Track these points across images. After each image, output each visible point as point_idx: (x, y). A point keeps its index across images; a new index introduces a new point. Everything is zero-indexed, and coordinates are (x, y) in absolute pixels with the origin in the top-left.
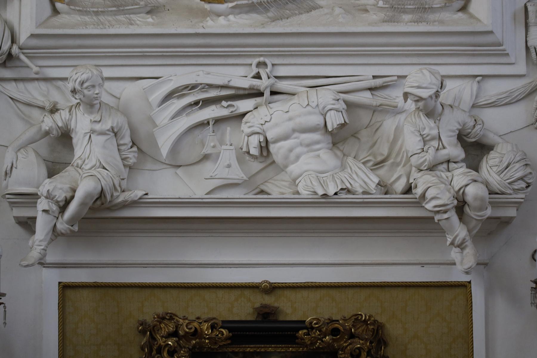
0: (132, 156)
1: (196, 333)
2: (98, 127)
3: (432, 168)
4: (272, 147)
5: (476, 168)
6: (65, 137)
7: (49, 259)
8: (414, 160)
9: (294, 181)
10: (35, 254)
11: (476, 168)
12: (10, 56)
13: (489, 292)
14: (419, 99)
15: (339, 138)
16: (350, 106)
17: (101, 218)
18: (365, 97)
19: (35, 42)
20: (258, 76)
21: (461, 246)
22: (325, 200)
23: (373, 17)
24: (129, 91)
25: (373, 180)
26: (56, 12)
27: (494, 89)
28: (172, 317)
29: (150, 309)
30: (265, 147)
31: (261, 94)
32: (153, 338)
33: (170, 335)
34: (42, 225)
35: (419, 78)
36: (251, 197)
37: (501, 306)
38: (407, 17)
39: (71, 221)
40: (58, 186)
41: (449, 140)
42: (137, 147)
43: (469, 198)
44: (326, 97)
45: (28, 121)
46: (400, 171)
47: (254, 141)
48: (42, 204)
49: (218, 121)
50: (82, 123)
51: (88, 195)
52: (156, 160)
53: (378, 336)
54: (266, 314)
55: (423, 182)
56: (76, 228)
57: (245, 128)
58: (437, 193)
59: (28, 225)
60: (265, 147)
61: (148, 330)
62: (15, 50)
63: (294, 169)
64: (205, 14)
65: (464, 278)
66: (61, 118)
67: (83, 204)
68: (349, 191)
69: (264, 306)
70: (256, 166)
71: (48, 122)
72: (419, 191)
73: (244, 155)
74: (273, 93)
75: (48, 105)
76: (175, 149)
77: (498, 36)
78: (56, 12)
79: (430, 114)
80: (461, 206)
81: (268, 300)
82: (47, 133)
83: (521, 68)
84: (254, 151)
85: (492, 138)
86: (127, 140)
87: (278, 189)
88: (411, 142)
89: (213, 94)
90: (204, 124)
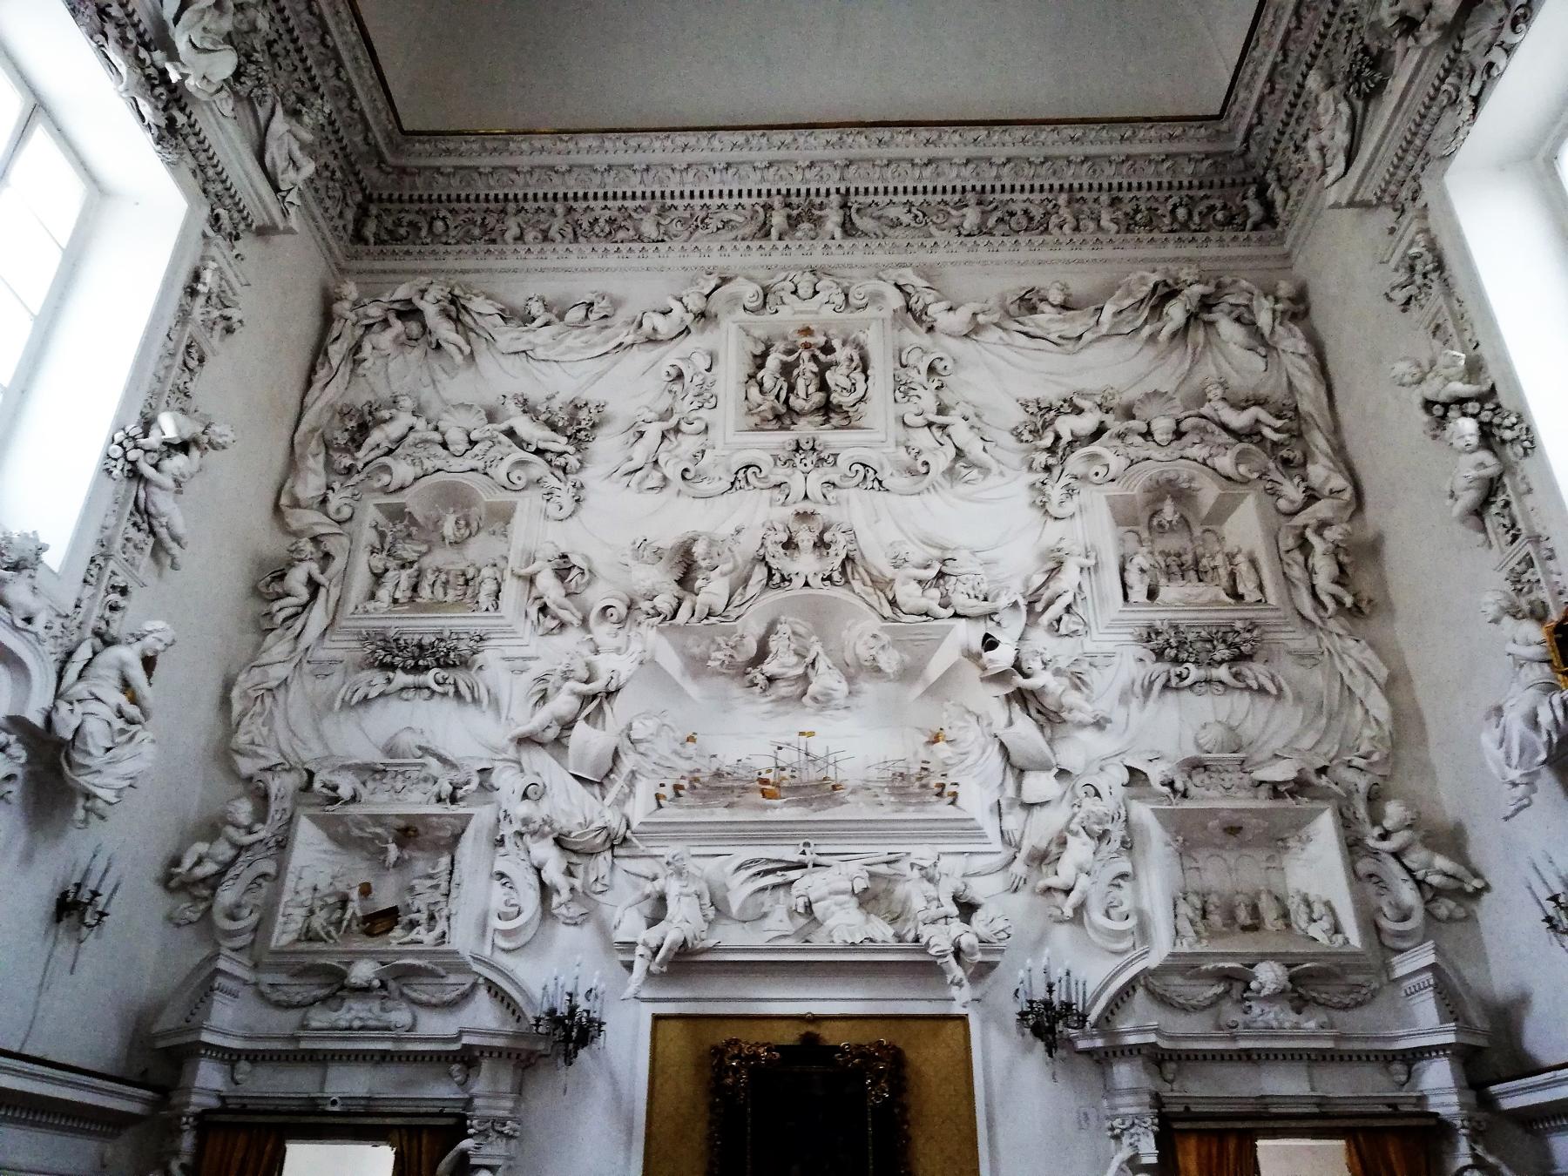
0: (711, 913)
1: (756, 1056)
2: (685, 890)
3: (934, 922)
4: (814, 907)
5: (968, 923)
6: (662, 899)
7: (644, 994)
8: (920, 916)
9: (830, 934)
10: (630, 991)
11: (968, 923)
12: (625, 839)
13: (984, 1022)
14: (922, 868)
15: (867, 900)
16: (872, 876)
17: (684, 962)
18: (883, 869)
19: (643, 828)
20: (804, 853)
21: (959, 984)
22: (853, 948)
23: (887, 809)
24: (710, 865)
25: (890, 931)
26: (660, 806)
27: (978, 863)
28: (737, 1041)
29: (723, 1035)
30: (809, 907)
31: (805, 866)
32: (721, 1061)
33: (733, 1058)
34: (640, 966)
35: (923, 852)
36: (800, 945)
37: (994, 1034)
38: (911, 809)
39: (661, 964)
40: (653, 936)
41: (947, 901)
42: (718, 907)
43: (963, 945)
44: (854, 867)
45: (636, 887)
46: (910, 925)
47: (801, 902)
48: (640, 950)
49: (775, 887)
50: (673, 888)
51: (674, 943)
52: (729, 917)
53: (896, 1058)
54: (810, 1040)
55: (926, 933)
56: (665, 969)
57: (795, 890)
58: (939, 939)
59: (629, 966)
60: (809, 907)
61: (718, 1052)
62: (629, 834)
63: (830, 923)
64: (765, 808)
65: (962, 1011)
66: (658, 885)
67: (670, 950)
68: (871, 940)
69: (808, 1034)
70: (802, 921)
71: (649, 888)
72: (923, 941)
73: (792, 913)
74: (815, 865)
75: (651, 875)
76: (743, 908)
77: (980, 821)
78: (660, 806)
79: (931, 880)
80: (958, 952)
81: (811, 1028)
82: (648, 896)
83: (997, 845)
84: (801, 910)
85: (979, 899)
86: (707, 900)
87: (819, 940)
88: (918, 903)
89: (771, 866)
90: (764, 889)
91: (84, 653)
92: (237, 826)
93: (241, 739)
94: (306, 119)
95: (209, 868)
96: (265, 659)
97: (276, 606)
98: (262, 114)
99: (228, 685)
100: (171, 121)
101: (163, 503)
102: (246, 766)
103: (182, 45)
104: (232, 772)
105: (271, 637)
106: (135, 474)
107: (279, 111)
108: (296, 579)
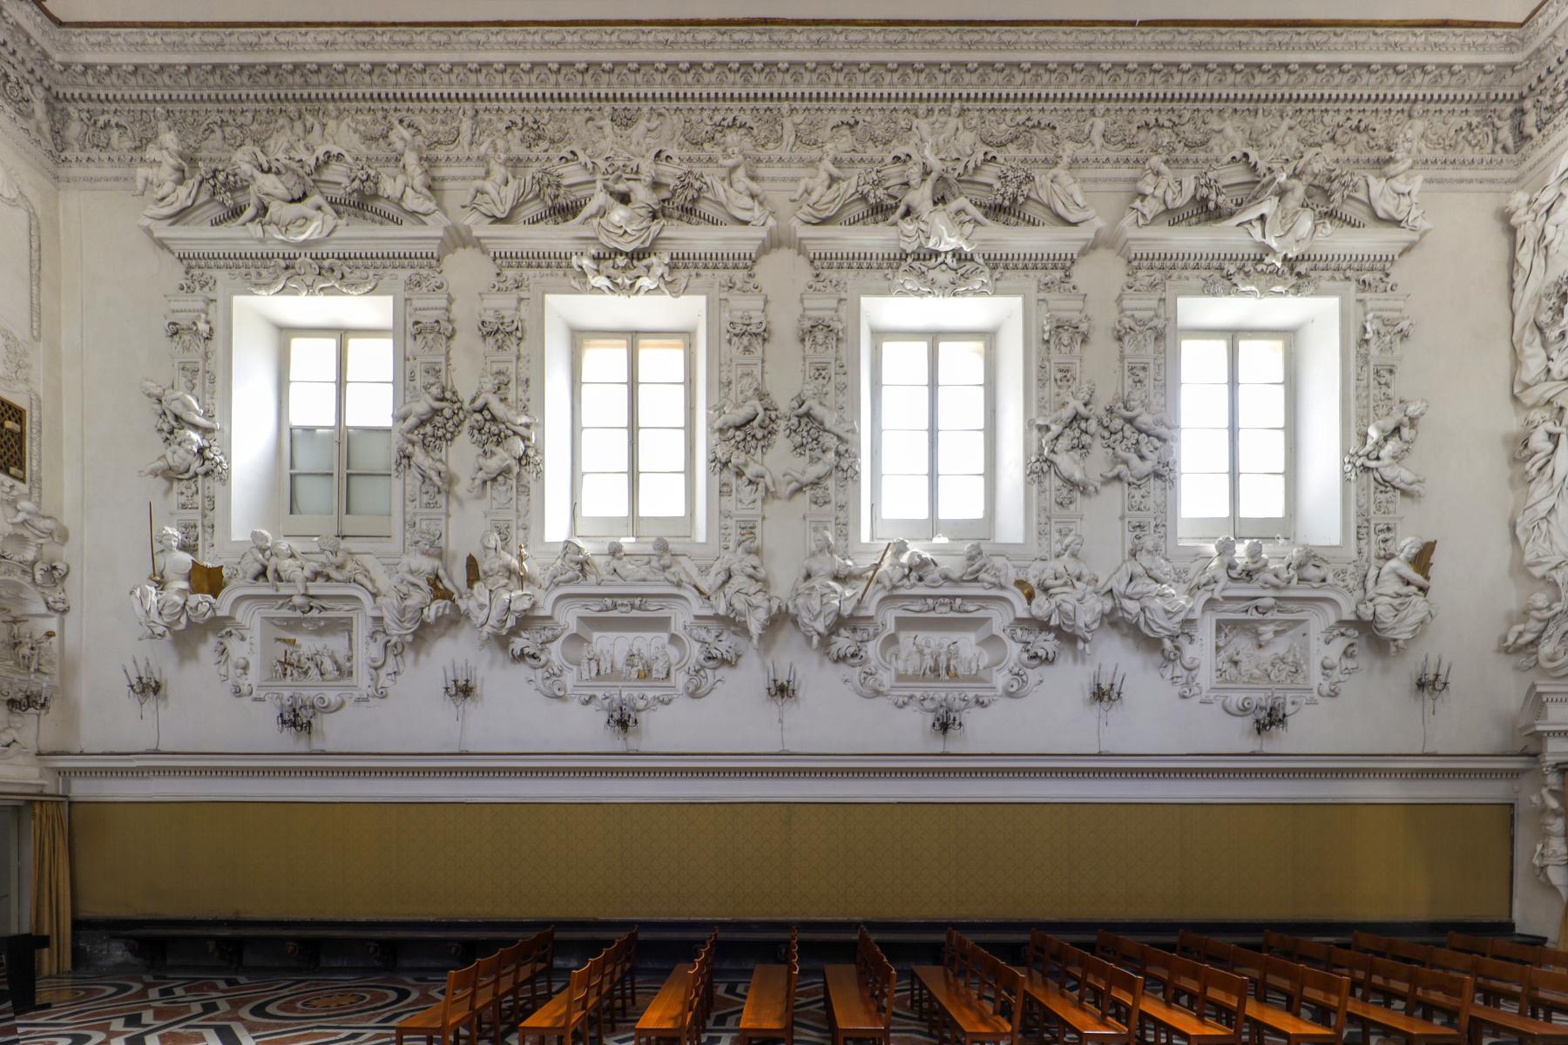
91: (1373, 573)
92: (1539, 609)
93: (1529, 558)
94: (1398, 156)
95: (1528, 637)
96: (1531, 502)
97: (1528, 465)
98: (1361, 195)
99: (1513, 526)
100: (1299, 274)
101: (1389, 473)
102: (1538, 572)
103: (1274, 244)
104: (1531, 577)
105: (1533, 486)
106: (1367, 469)
107: (1372, 180)
108: (1539, 441)
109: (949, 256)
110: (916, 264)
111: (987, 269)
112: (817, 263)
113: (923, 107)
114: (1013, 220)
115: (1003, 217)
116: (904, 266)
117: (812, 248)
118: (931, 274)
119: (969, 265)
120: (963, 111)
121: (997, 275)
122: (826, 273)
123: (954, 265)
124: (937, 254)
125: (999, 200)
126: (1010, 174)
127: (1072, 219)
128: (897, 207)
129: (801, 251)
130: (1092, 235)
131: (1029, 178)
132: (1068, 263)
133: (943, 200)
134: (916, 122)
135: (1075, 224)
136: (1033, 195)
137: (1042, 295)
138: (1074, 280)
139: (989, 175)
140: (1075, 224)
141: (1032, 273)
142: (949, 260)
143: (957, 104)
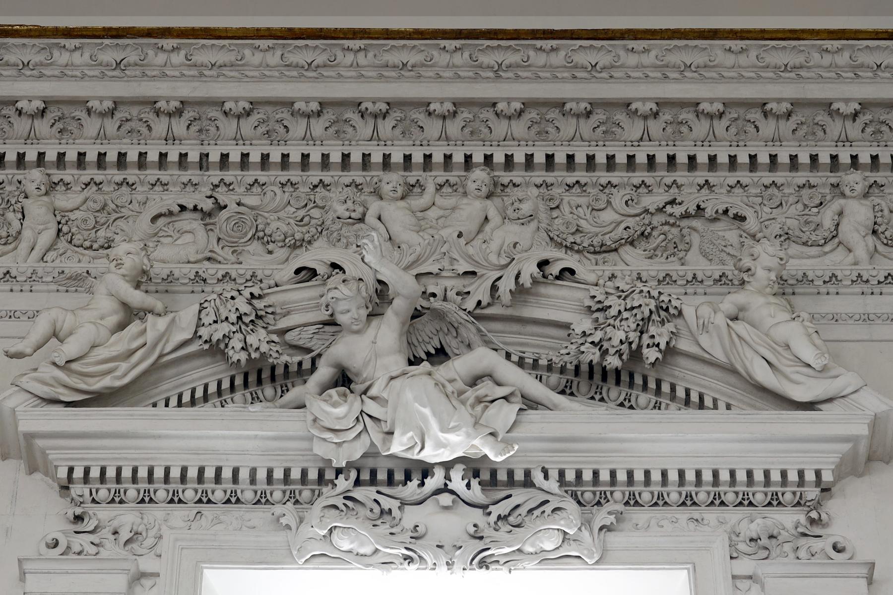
109: (457, 475)
110: (365, 494)
111: (570, 505)
112: (77, 489)
113: (392, 181)
114: (643, 398)
115: (615, 393)
116: (330, 495)
117: (62, 459)
118: (411, 516)
119: (519, 496)
120: (495, 191)
121: (602, 517)
122: (103, 513)
123: (476, 493)
124: (426, 471)
125: (593, 355)
126: (616, 305)
127: (800, 394)
128: (314, 368)
129: (35, 464)
130: (863, 430)
131: (666, 312)
132: (812, 493)
133: (440, 355)
134: (375, 206)
135: (810, 406)
136: (684, 345)
137: (744, 566)
138: (837, 532)
139: (560, 304)
140: (810, 406)
141: (712, 515)
142: (457, 483)
143: (480, 175)
